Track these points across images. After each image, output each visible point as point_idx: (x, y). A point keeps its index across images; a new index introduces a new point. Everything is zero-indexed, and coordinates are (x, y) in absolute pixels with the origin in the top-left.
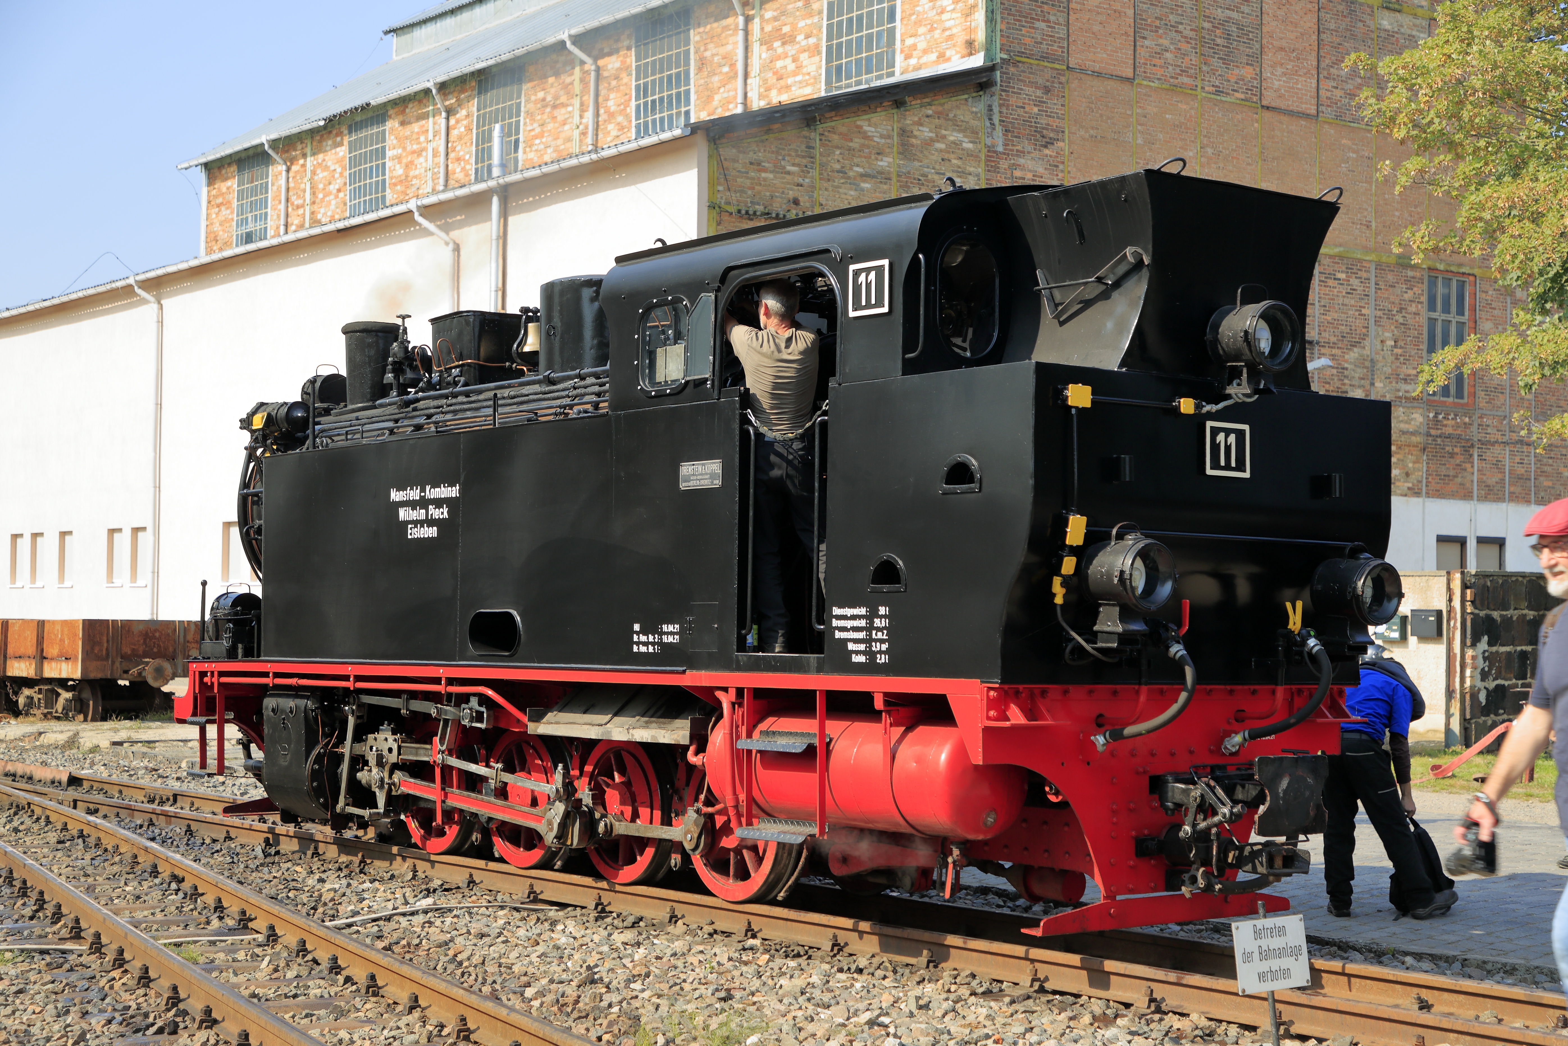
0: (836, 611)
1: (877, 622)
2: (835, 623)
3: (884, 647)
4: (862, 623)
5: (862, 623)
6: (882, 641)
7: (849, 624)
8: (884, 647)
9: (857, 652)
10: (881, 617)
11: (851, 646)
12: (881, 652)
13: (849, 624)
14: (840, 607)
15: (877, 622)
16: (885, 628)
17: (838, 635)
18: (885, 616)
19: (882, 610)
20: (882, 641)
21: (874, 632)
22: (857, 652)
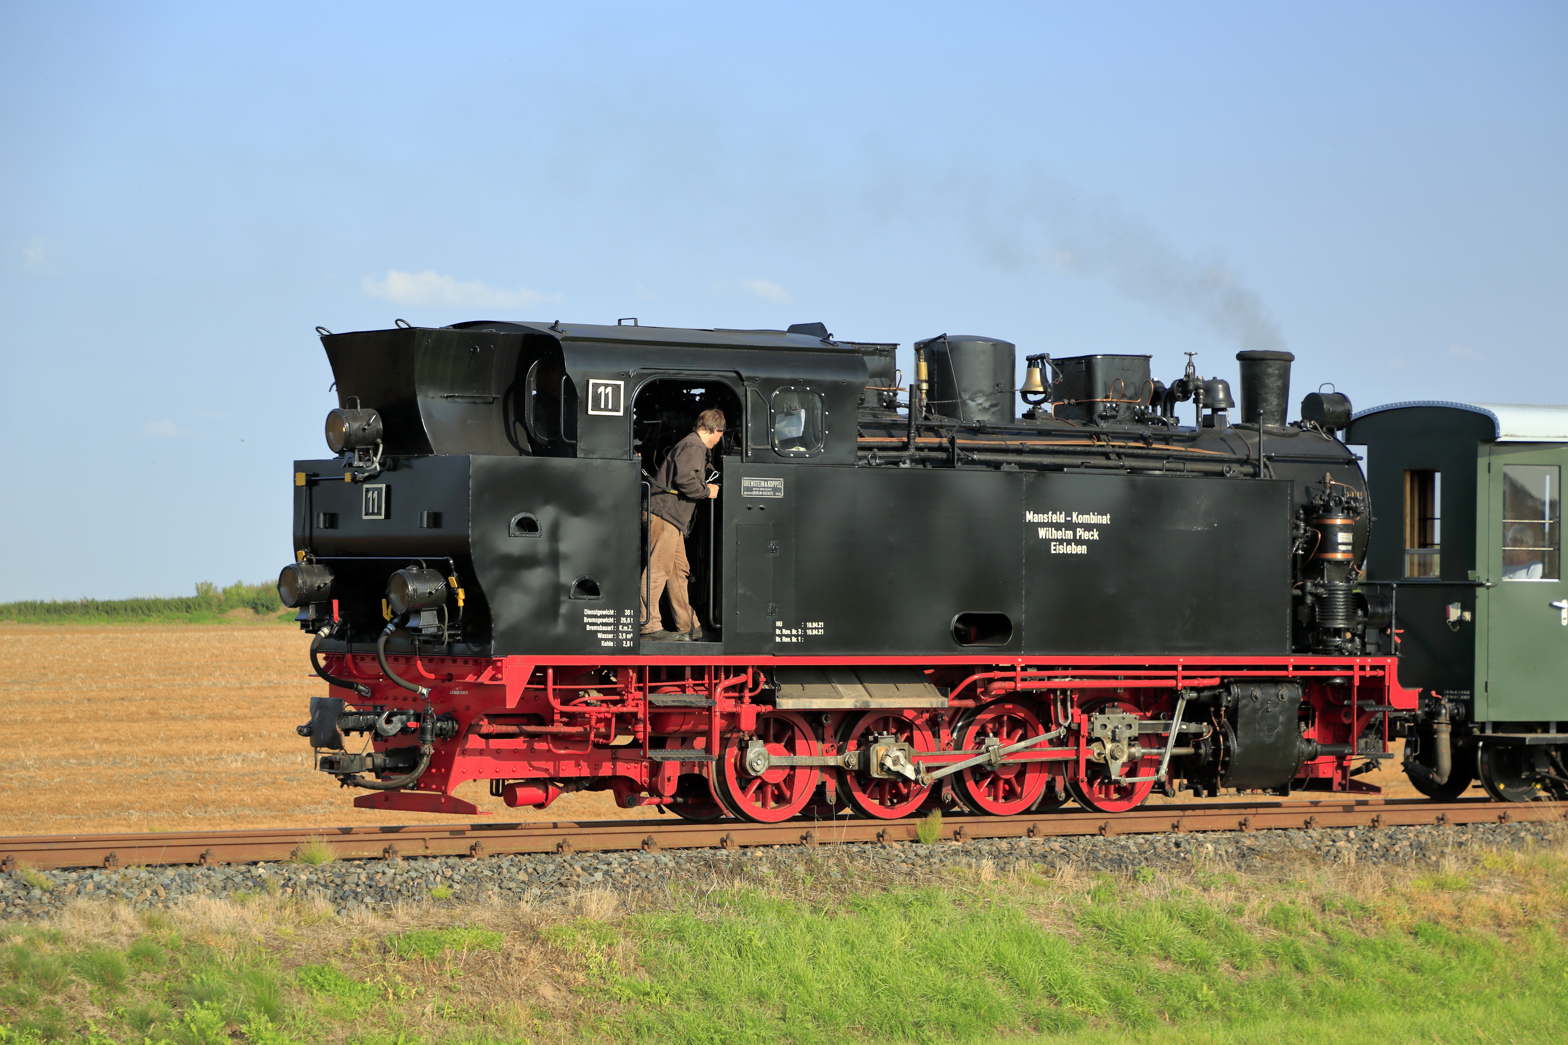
0: (587, 612)
1: (623, 620)
2: (586, 620)
3: (629, 636)
4: (611, 620)
5: (611, 620)
6: (627, 633)
7: (599, 621)
8: (629, 636)
9: (606, 640)
10: (627, 617)
11: (600, 636)
12: (626, 640)
13: (599, 621)
14: (590, 609)
15: (623, 620)
16: (630, 624)
17: (588, 628)
18: (630, 616)
19: (627, 612)
20: (627, 633)
21: (620, 627)
22: (606, 640)
